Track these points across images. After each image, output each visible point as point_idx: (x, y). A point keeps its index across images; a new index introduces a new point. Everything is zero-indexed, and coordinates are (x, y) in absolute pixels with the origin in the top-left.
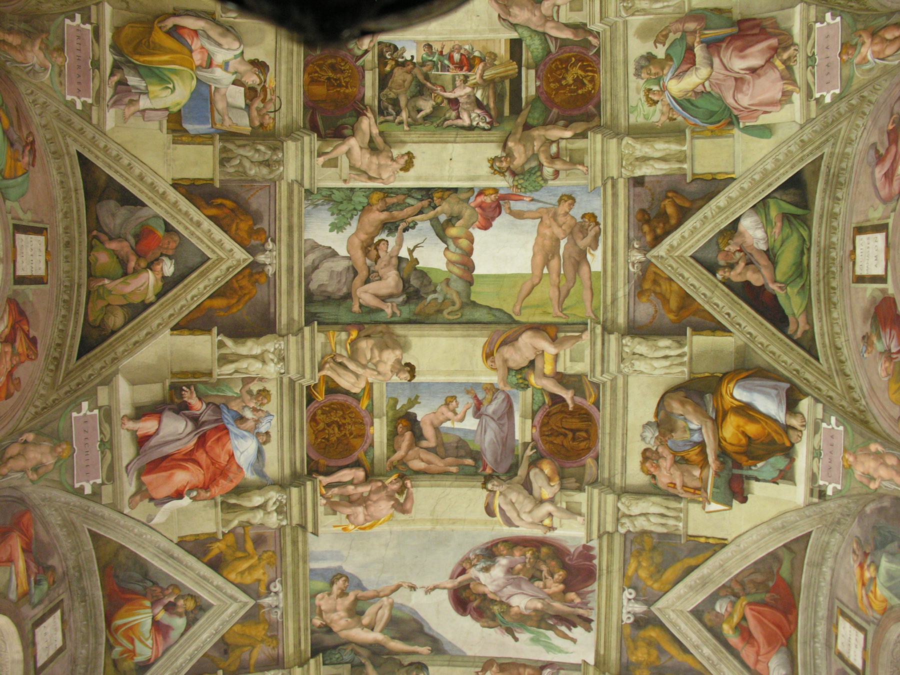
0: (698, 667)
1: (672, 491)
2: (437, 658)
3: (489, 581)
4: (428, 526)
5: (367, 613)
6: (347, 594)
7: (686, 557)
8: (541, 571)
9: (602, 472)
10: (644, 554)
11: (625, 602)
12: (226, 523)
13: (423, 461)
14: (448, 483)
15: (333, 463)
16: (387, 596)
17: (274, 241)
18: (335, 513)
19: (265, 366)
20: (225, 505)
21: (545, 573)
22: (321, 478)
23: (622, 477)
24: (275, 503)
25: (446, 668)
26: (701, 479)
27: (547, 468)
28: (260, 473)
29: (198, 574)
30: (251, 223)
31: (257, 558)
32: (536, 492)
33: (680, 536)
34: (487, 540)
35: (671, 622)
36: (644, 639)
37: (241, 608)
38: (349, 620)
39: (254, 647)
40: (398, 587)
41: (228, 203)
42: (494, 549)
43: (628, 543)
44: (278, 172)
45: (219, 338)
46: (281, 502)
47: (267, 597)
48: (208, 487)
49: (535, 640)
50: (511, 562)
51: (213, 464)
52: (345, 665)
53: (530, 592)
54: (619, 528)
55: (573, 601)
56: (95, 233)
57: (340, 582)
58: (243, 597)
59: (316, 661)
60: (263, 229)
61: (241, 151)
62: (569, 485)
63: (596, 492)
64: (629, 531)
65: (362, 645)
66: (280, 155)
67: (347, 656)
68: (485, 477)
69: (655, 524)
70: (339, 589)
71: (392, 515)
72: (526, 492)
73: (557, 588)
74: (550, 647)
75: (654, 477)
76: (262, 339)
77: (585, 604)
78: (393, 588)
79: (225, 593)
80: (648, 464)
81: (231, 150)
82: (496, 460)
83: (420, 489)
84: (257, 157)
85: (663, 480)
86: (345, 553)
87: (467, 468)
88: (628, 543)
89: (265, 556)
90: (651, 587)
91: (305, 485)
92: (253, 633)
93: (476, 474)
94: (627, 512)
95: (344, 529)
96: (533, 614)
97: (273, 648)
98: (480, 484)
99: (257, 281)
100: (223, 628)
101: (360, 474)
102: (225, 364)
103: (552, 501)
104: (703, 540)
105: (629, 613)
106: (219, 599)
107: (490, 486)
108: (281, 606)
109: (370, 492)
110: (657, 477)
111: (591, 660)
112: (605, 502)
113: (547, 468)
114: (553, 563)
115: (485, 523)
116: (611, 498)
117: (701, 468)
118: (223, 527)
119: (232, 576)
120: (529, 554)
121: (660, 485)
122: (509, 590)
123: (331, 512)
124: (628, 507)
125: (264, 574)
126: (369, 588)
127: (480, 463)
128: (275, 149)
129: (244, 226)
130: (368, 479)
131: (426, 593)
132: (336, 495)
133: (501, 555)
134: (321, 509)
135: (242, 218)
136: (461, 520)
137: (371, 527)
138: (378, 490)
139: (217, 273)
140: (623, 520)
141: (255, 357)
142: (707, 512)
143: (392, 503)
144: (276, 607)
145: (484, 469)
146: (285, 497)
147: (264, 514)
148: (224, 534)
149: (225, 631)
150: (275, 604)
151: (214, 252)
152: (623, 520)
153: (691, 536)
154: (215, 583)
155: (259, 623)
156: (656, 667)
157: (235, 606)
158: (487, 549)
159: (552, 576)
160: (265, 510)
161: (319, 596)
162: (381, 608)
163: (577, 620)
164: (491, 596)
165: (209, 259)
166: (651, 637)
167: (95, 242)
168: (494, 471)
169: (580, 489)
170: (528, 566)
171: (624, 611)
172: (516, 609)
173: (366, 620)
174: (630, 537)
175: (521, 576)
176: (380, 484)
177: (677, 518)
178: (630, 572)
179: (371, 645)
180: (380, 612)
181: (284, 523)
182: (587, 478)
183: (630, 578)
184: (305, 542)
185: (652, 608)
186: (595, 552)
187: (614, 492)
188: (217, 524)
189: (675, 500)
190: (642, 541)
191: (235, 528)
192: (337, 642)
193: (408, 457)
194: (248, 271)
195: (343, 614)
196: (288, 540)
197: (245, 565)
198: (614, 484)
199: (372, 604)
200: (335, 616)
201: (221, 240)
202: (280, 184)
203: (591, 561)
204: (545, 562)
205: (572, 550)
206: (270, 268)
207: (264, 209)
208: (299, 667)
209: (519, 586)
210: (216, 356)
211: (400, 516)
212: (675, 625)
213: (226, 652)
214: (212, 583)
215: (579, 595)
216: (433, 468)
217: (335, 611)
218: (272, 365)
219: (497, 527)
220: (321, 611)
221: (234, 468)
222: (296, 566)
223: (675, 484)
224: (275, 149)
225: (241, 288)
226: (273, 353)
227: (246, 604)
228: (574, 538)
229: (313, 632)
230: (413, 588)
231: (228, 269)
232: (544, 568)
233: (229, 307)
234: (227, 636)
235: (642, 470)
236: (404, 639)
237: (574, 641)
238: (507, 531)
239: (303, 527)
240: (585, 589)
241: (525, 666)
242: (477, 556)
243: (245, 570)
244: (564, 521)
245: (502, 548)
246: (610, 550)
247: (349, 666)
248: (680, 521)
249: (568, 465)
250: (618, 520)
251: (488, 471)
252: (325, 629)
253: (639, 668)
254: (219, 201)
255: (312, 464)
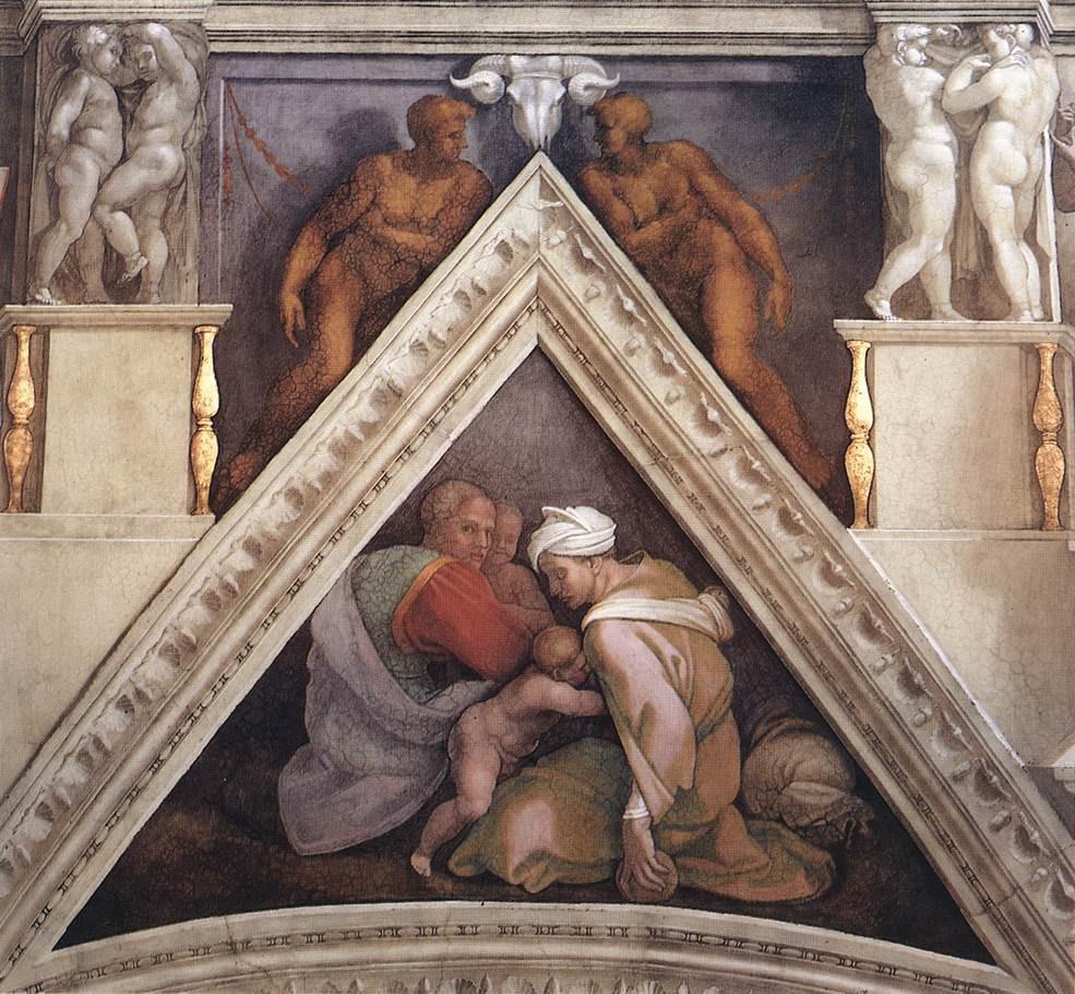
17: (465, 65)
19: (1007, 109)
30: (385, 163)
41: (301, 262)
44: (171, 45)
45: (884, 308)
56: (421, 863)
60: (415, 111)
61: (78, 205)
66: (97, 35)
76: (888, 118)
81: (73, 254)
84: (104, 136)
99: (638, 139)
102: (998, 288)
128: (73, 60)
129: (400, 193)
135: (364, 200)
139: (602, 319)
141: (966, 151)
151: (510, 330)
165: (540, 351)
167: (462, 867)
194: (596, 180)
201: (460, 295)
202: (221, 35)
206: (579, 82)
207: (325, 104)
210: (963, 323)
218: (997, 77)
224: (73, 60)
225: (664, 207)
226: (947, 71)
231: (586, 265)
233: (750, 260)
254: (291, 302)
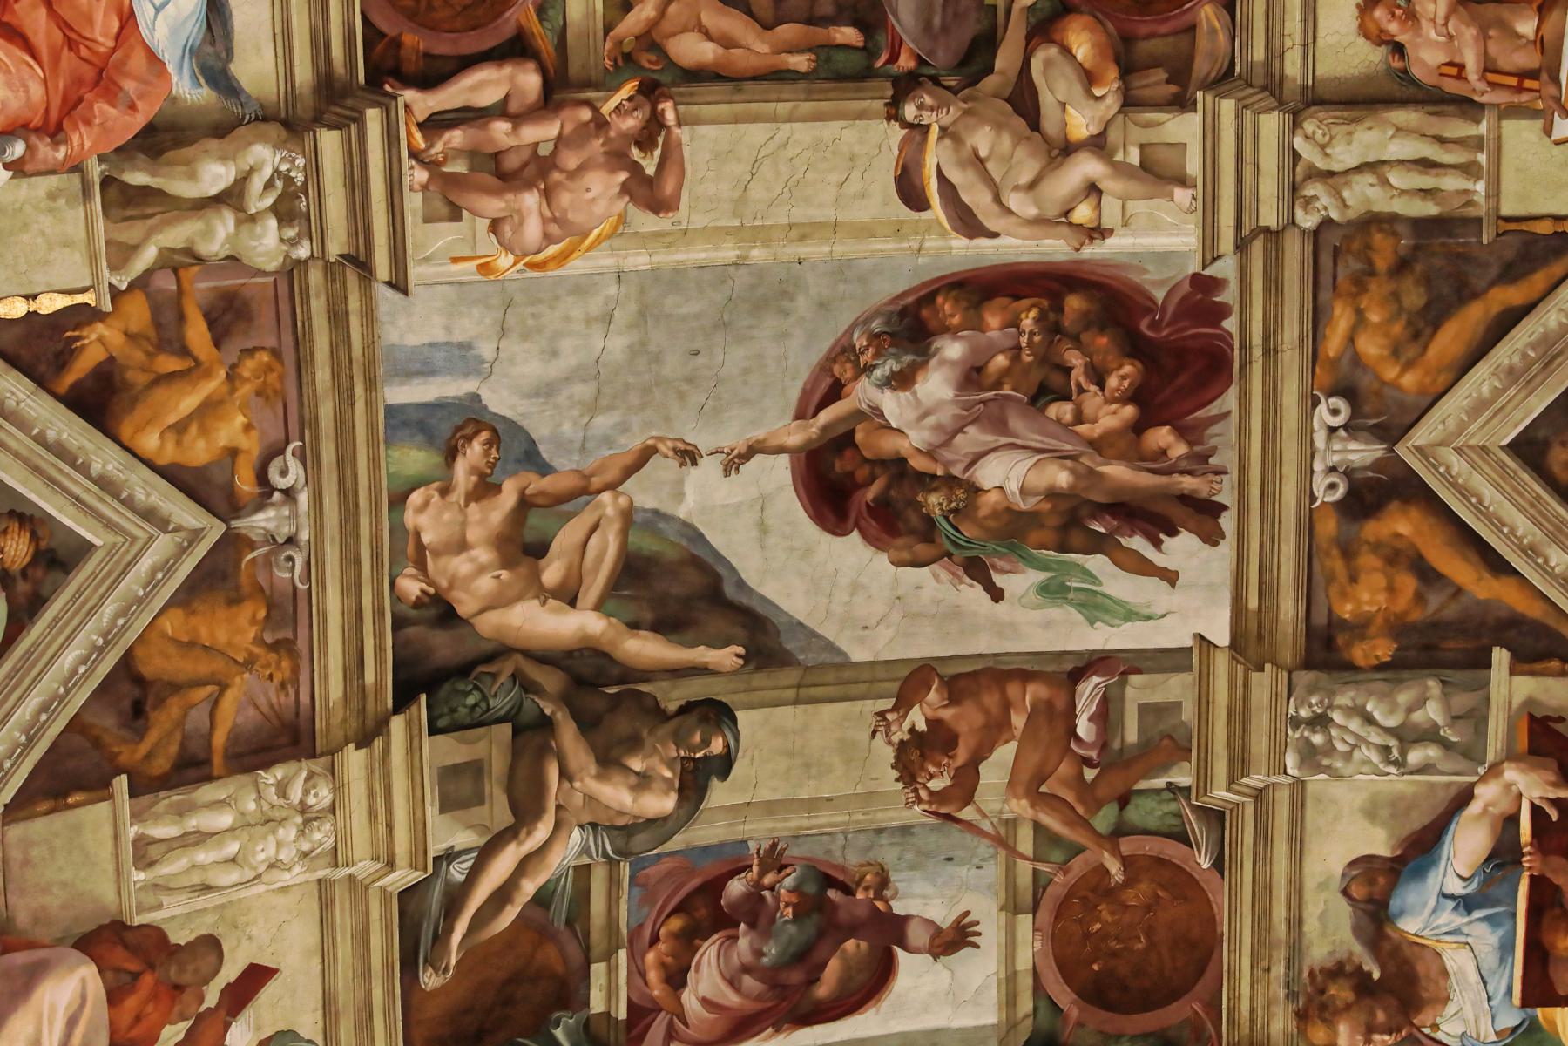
0: (1534, 611)
1: (1451, 86)
2: (759, 679)
3: (911, 415)
4: (728, 253)
5: (555, 547)
6: (497, 489)
7: (1493, 284)
8: (1068, 371)
9: (1247, 45)
10: (1373, 286)
11: (1320, 439)
12: (121, 254)
13: (708, 36)
14: (783, 108)
15: (444, 46)
16: (612, 486)
18: (455, 215)
20: (113, 192)
21: (1078, 375)
22: (409, 95)
23: (1304, 57)
24: (269, 185)
25: (789, 709)
26: (1540, 42)
27: (1082, 42)
28: (217, 75)
29: (41, 440)
31: (222, 374)
32: (1050, 123)
33: (1479, 220)
34: (902, 287)
35: (1454, 485)
36: (1376, 547)
37: (182, 551)
38: (505, 574)
39: (223, 687)
40: (646, 455)
42: (925, 313)
43: (1326, 260)
46: (289, 180)
47: (260, 507)
48: (59, 128)
49: (1052, 591)
50: (974, 350)
51: (71, 45)
52: (495, 727)
53: (1036, 440)
54: (1299, 213)
55: (1164, 452)
57: (476, 449)
58: (186, 513)
59: (409, 723)
62: (1146, 93)
63: (1228, 107)
64: (1327, 222)
65: (545, 658)
67: (500, 703)
68: (896, 81)
69: (1403, 192)
70: (474, 470)
71: (622, 219)
72: (1020, 123)
73: (1110, 417)
74: (1095, 607)
75: (1399, 49)
77: (1200, 461)
78: (628, 460)
79: (128, 503)
80: (1379, 13)
82: (927, 26)
83: (703, 130)
85: (1427, 57)
86: (486, 350)
87: (840, 57)
88: (1326, 260)
89: (249, 367)
90: (1394, 385)
91: (360, 121)
92: (222, 636)
93: (865, 74)
94: (1321, 164)
95: (485, 269)
96: (1047, 506)
97: (283, 686)
98: (879, 105)
100: (124, 629)
101: (530, 81)
103: (1098, 144)
104: (1545, 228)
105: (1333, 469)
106: (110, 525)
107: (910, 111)
108: (304, 536)
109: (559, 138)
110: (1409, 49)
111: (1221, 636)
112: (1256, 137)
113: (1082, 42)
114: (1103, 341)
115: (898, 231)
116: (1271, 124)
117: (1540, 10)
118: (114, 268)
119: (150, 442)
120: (1028, 322)
121: (1416, 72)
122: (974, 437)
123: (444, 210)
124: (1323, 147)
125: (248, 428)
126: (556, 463)
127: (882, 39)
130: (552, 97)
131: (727, 473)
132: (459, 153)
133: (946, 330)
134: (413, 203)
136: (822, 225)
137: (562, 258)
138: (583, 134)
140: (1310, 190)
142: (1557, 143)
143: (623, 176)
144: (291, 541)
145: (893, 58)
146: (300, 162)
147: (239, 223)
148: (116, 294)
149: (131, 636)
150: (286, 530)
152: (1310, 190)
153: (1508, 219)
154: (96, 468)
155: (234, 601)
156: (1412, 628)
157: (163, 545)
158: (903, 313)
159: (1101, 384)
160: (239, 208)
161: (416, 498)
162: (594, 528)
163: (1176, 512)
164: (918, 463)
166: (1398, 536)
168: (921, 61)
169: (1182, 103)
170: (1027, 358)
171: (1318, 466)
172: (993, 497)
173: (552, 573)
174: (1334, 238)
175: (1007, 391)
176: (585, 114)
177: (1470, 170)
178: (1333, 344)
179: (570, 654)
180: (594, 541)
181: (303, 252)
182: (1202, 67)
183: (1334, 363)
184: (369, 315)
185: (1401, 450)
186: (1229, 296)
187: (1281, 105)
188: (93, 258)
189: (1464, 115)
190: (1368, 247)
191: (148, 273)
192: (468, 650)
193: (666, 26)
195: (484, 555)
196: (318, 305)
197: (189, 402)
198: (1283, 77)
199: (569, 516)
200: (460, 565)
203: (1217, 324)
204: (1076, 341)
205: (1159, 295)
208: (358, 747)
209: (1000, 426)
211: (646, 222)
212: (1464, 492)
213: (137, 712)
214: (84, 470)
215: (1182, 432)
216: (740, 59)
217: (462, 546)
219: (932, 243)
220: (420, 547)
221: (138, 62)
222: (345, 398)
223: (1461, 67)
227: (196, 535)
228: (1164, 257)
229: (399, 623)
230: (689, 456)
232: (1075, 359)
234: (140, 653)
235: (1364, 31)
236: (668, 625)
237: (1170, 577)
238: (962, 253)
239: (360, 262)
240: (1201, 413)
241: (1025, 676)
242: (874, 337)
243: (190, 418)
244: (1135, 207)
245: (947, 307)
246: (1274, 285)
247: (506, 729)
248: (1478, 178)
249: (1143, 30)
250: (1294, 188)
251: (905, 62)
252: (432, 612)
253: (1362, 638)
255: (380, 47)
